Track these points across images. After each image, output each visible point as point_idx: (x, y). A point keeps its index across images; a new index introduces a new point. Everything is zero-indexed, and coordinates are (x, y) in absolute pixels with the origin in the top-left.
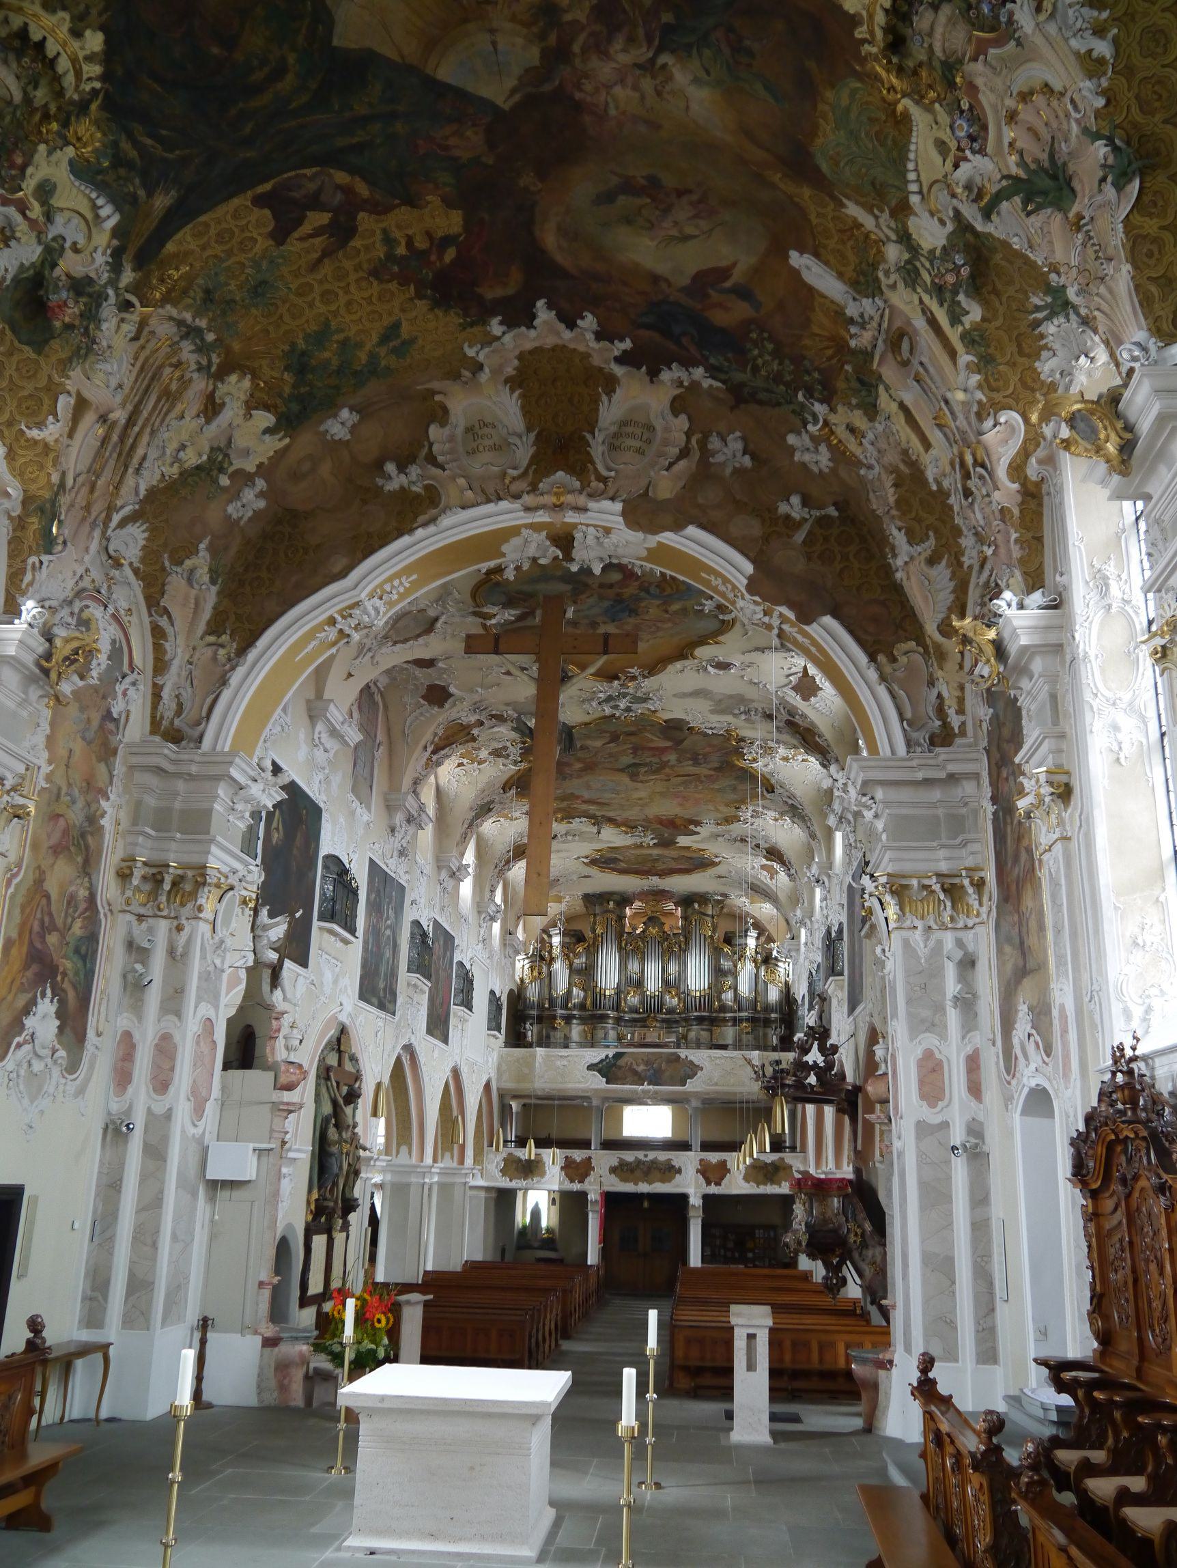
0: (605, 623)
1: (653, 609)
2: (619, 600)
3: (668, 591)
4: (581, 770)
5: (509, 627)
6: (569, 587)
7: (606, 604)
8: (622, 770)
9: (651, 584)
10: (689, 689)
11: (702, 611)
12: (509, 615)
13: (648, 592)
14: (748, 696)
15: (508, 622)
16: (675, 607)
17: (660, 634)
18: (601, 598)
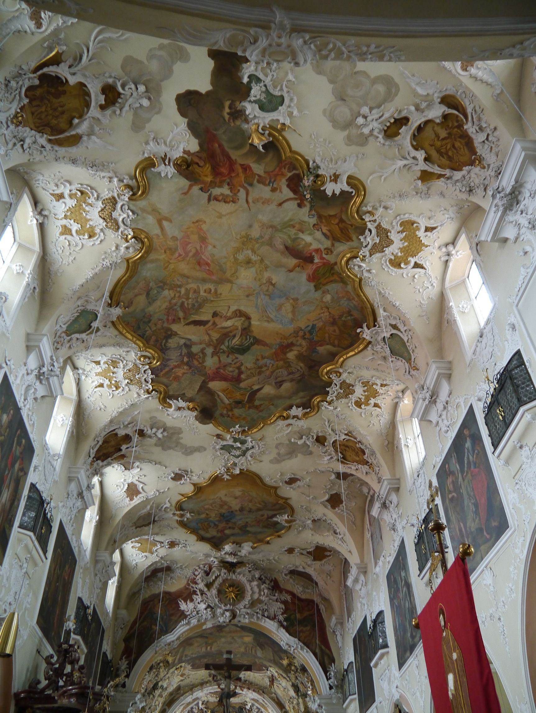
0: (236, 511)
1: (213, 516)
2: (228, 521)
3: (206, 524)
4: (290, 346)
5: (283, 511)
6: (248, 529)
7: (233, 520)
8: (257, 341)
9: (213, 528)
10: (196, 454)
11: (190, 513)
12: (278, 519)
13: (215, 524)
14: (160, 448)
15: (281, 514)
16: (203, 516)
17: (211, 502)
18: (235, 523)
